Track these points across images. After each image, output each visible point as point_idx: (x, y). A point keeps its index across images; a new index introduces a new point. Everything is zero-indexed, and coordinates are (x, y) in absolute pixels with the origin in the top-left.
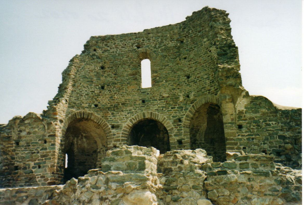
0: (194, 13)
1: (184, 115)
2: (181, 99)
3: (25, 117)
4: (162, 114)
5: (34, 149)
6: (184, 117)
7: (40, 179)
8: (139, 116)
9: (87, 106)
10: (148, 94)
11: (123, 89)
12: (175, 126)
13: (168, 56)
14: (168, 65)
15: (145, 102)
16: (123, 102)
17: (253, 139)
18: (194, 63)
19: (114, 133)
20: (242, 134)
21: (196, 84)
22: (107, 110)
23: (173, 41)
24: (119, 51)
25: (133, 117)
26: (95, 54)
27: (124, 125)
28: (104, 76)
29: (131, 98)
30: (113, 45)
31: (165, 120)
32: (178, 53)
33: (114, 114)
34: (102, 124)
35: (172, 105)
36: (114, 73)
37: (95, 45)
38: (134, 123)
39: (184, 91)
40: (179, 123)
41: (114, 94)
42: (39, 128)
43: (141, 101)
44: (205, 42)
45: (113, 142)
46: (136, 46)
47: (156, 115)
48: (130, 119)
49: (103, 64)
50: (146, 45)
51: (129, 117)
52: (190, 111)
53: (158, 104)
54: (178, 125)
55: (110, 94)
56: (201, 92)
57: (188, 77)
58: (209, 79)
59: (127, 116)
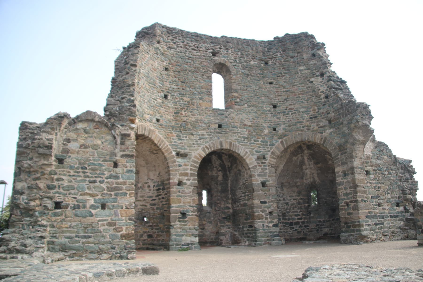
0: (287, 35)
1: (269, 151)
2: (266, 131)
3: (78, 117)
4: (244, 147)
5: (94, 176)
6: (270, 153)
7: (106, 227)
8: (214, 145)
9: (149, 119)
10: (226, 117)
11: (194, 105)
12: (259, 163)
13: (250, 76)
14: (251, 86)
15: (223, 127)
16: (193, 121)
17: (379, 188)
18: (284, 92)
19: (180, 164)
20: (370, 181)
21: (286, 117)
22: (171, 130)
23: (255, 60)
24: (188, 53)
25: (207, 145)
26: (158, 48)
28: (168, 81)
29: (204, 119)
30: (182, 44)
31: (247, 155)
32: (261, 76)
33: (180, 136)
34: (164, 148)
35: (255, 137)
36: (182, 80)
38: (207, 153)
39: (269, 122)
40: (264, 161)
41: (181, 109)
42: (103, 140)
44: (301, 70)
45: (178, 177)
46: (212, 53)
47: (236, 146)
48: (202, 146)
49: (167, 64)
51: (201, 144)
53: (239, 133)
54: (262, 163)
55: (175, 108)
56: (294, 127)
57: (275, 107)
58: (308, 114)
59: (199, 142)
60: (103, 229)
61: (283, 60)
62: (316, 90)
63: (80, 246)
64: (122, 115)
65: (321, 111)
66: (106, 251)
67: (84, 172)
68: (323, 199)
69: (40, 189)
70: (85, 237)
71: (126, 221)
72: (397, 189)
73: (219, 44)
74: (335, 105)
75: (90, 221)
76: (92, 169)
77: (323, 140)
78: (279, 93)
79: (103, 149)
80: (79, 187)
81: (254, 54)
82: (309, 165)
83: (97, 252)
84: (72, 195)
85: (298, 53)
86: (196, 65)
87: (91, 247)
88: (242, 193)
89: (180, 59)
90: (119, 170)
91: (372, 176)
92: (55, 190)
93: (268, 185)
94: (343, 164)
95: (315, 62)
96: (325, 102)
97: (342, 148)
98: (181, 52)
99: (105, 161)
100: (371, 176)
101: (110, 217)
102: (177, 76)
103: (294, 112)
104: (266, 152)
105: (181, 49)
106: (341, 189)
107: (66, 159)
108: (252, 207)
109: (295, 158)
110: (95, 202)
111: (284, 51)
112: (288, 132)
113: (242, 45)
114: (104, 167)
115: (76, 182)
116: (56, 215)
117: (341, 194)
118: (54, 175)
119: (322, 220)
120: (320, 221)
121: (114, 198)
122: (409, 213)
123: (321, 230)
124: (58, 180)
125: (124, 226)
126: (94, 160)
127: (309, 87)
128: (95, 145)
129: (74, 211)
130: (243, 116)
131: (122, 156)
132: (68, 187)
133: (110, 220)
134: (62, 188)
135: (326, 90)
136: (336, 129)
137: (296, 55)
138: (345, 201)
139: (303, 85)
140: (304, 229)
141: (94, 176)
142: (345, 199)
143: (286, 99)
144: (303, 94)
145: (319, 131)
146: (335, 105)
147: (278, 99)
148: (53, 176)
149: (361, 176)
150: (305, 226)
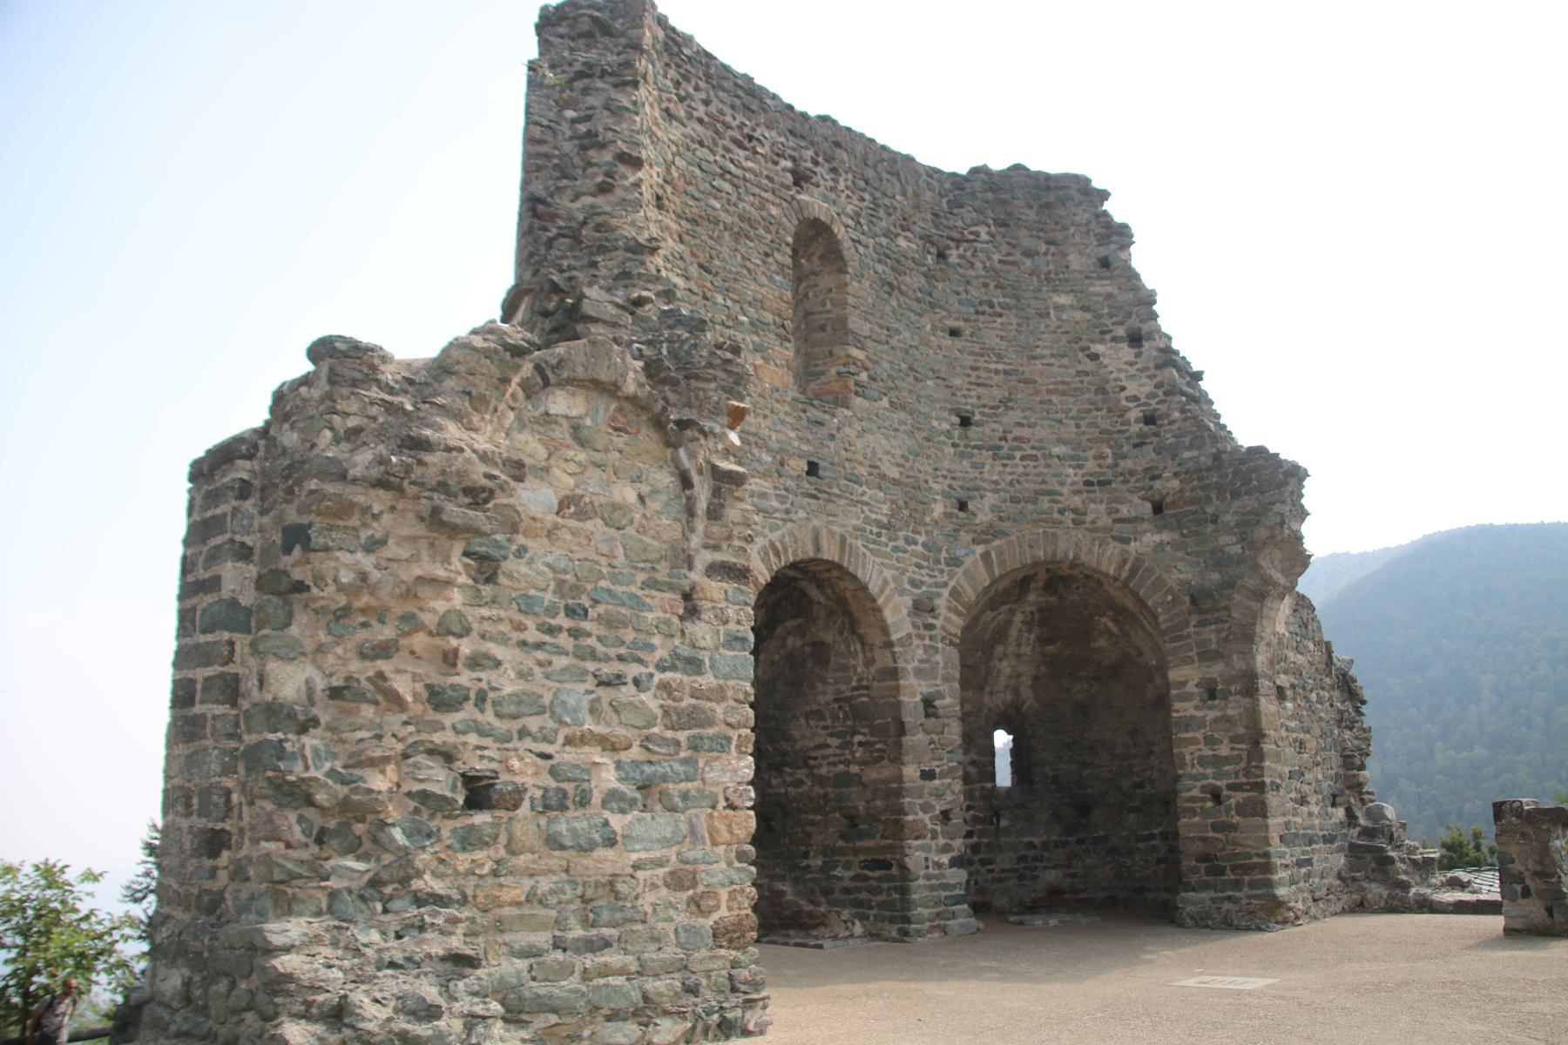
0: (1018, 168)
1: (945, 585)
2: (938, 509)
4: (878, 560)
5: (613, 652)
6: (946, 592)
7: (664, 891)
10: (832, 437)
14: (898, 332)
15: (821, 472)
18: (997, 372)
21: (1005, 466)
36: (702, 260)
39: (945, 477)
40: (931, 621)
44: (1060, 308)
46: (793, 172)
50: (822, 189)
53: (867, 504)
56: (1030, 507)
57: (965, 422)
58: (1080, 467)
60: (654, 905)
61: (996, 257)
62: (1109, 387)
63: (577, 991)
64: (704, 385)
65: (1128, 464)
66: (668, 1006)
67: (575, 633)
68: (1047, 769)
69: (396, 701)
70: (592, 946)
71: (730, 864)
73: (812, 143)
74: (1187, 454)
75: (609, 868)
76: (610, 622)
77: (1127, 567)
78: (983, 374)
79: (645, 533)
80: (564, 702)
81: (909, 210)
82: (1019, 645)
83: (635, 1014)
84: (535, 739)
85: (1048, 243)
86: (748, 208)
87: (617, 990)
88: (831, 735)
89: (697, 171)
90: (701, 631)
92: (460, 716)
93: (941, 711)
94: (1207, 656)
95: (1109, 289)
96: (1141, 435)
97: (1201, 601)
98: (701, 144)
99: (652, 584)
101: (675, 849)
102: (687, 238)
103: (1030, 452)
104: (937, 585)
105: (699, 128)
106: (1194, 741)
107: (505, 558)
108: (894, 792)
109: (989, 615)
110: (620, 780)
111: (1001, 224)
112: (1007, 524)
113: (875, 167)
114: (650, 616)
115: (547, 677)
116: (469, 840)
117: (1188, 758)
118: (460, 636)
119: (1036, 841)
120: (1031, 845)
121: (685, 761)
122: (1358, 829)
123: (1035, 878)
124: (476, 662)
125: (723, 885)
126: (615, 579)
127: (1087, 374)
128: (616, 507)
129: (543, 821)
130: (876, 442)
132: (520, 703)
133: (674, 859)
134: (494, 703)
135: (1151, 396)
136: (1183, 535)
137: (1043, 248)
138: (1205, 782)
139: (1065, 361)
140: (978, 872)
141: (613, 652)
142: (1205, 777)
143: (1006, 403)
144: (1063, 393)
145: (1115, 533)
146: (1187, 454)
147: (979, 398)
148: (454, 642)
150: (983, 862)
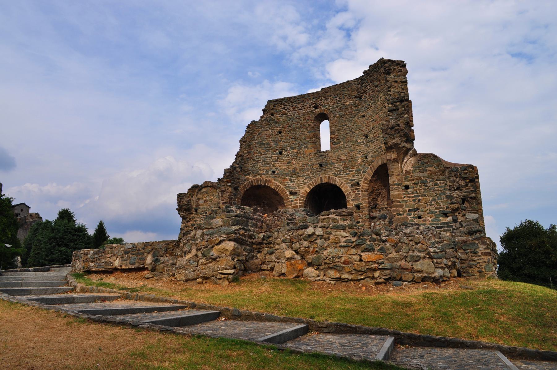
2: (360, 161)
6: (363, 180)
10: (325, 157)
17: (419, 200)
25: (311, 182)
27: (302, 191)
37: (273, 109)
43: (318, 165)
46: (314, 107)
52: (368, 174)
54: (356, 189)
72: (445, 199)
91: (410, 191)
100: (409, 190)
131: (223, 203)
149: (398, 191)
